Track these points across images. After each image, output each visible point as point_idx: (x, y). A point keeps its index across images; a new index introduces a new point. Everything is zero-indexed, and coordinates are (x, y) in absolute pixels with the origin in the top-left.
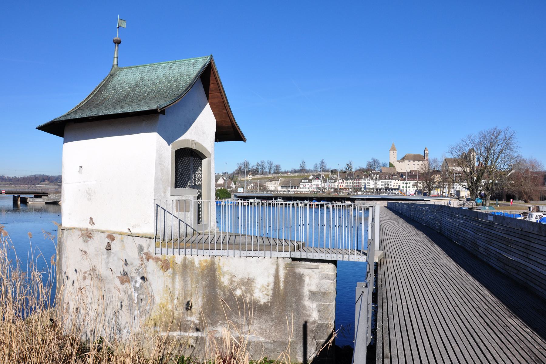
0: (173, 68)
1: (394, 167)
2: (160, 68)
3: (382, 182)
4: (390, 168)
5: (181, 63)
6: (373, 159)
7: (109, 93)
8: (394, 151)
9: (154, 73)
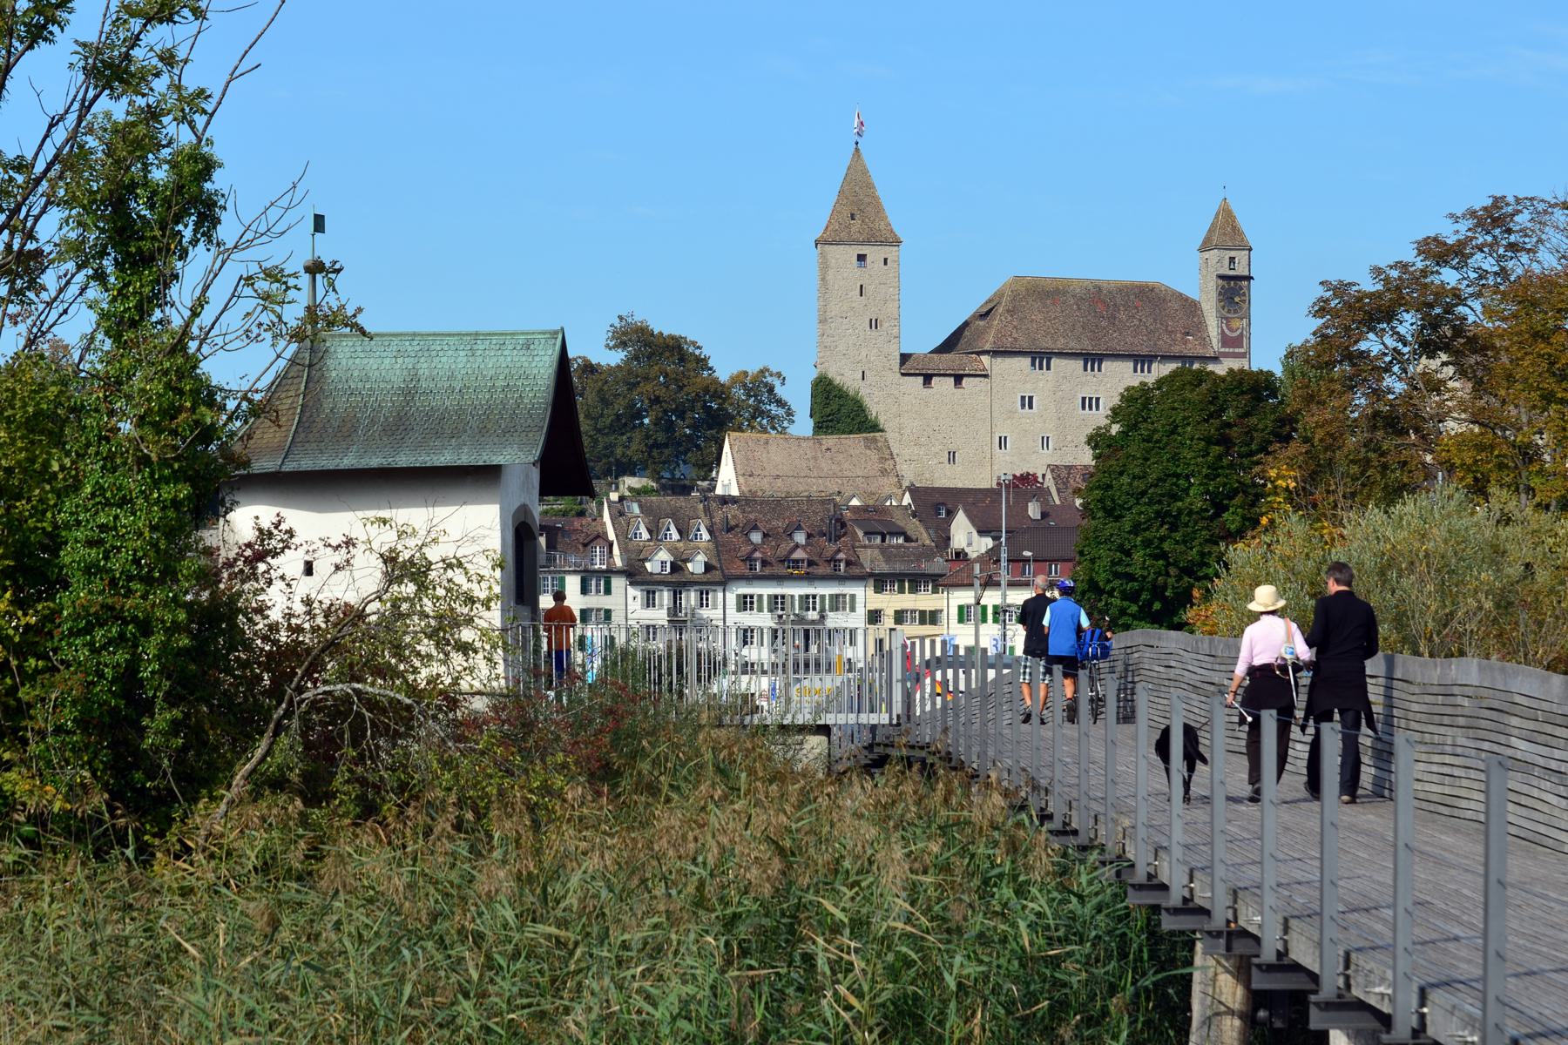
0: (479, 353)
1: (875, 427)
2: (446, 348)
3: (745, 603)
4: (830, 440)
5: (494, 342)
6: (634, 337)
7: (341, 406)
8: (874, 254)
9: (436, 360)
